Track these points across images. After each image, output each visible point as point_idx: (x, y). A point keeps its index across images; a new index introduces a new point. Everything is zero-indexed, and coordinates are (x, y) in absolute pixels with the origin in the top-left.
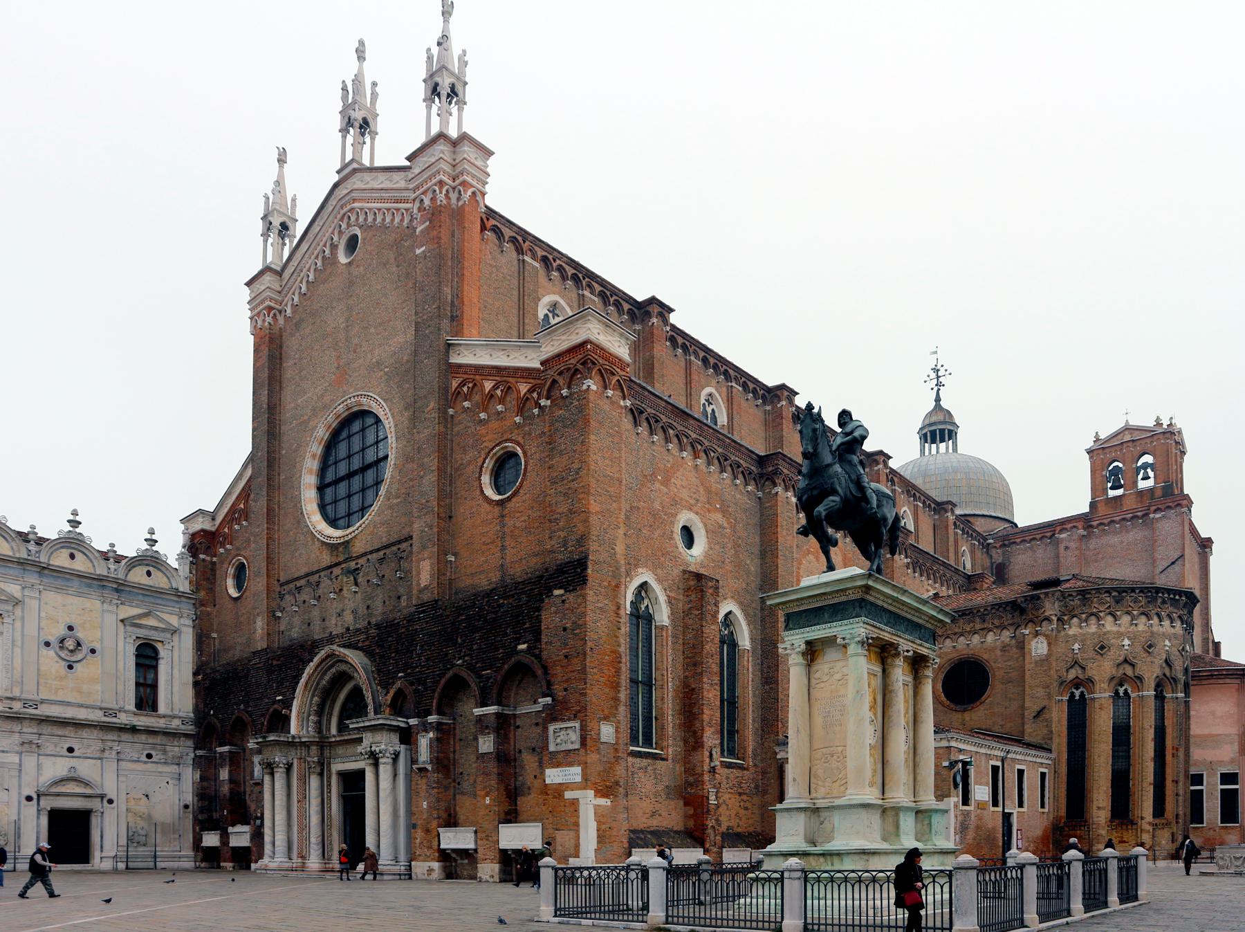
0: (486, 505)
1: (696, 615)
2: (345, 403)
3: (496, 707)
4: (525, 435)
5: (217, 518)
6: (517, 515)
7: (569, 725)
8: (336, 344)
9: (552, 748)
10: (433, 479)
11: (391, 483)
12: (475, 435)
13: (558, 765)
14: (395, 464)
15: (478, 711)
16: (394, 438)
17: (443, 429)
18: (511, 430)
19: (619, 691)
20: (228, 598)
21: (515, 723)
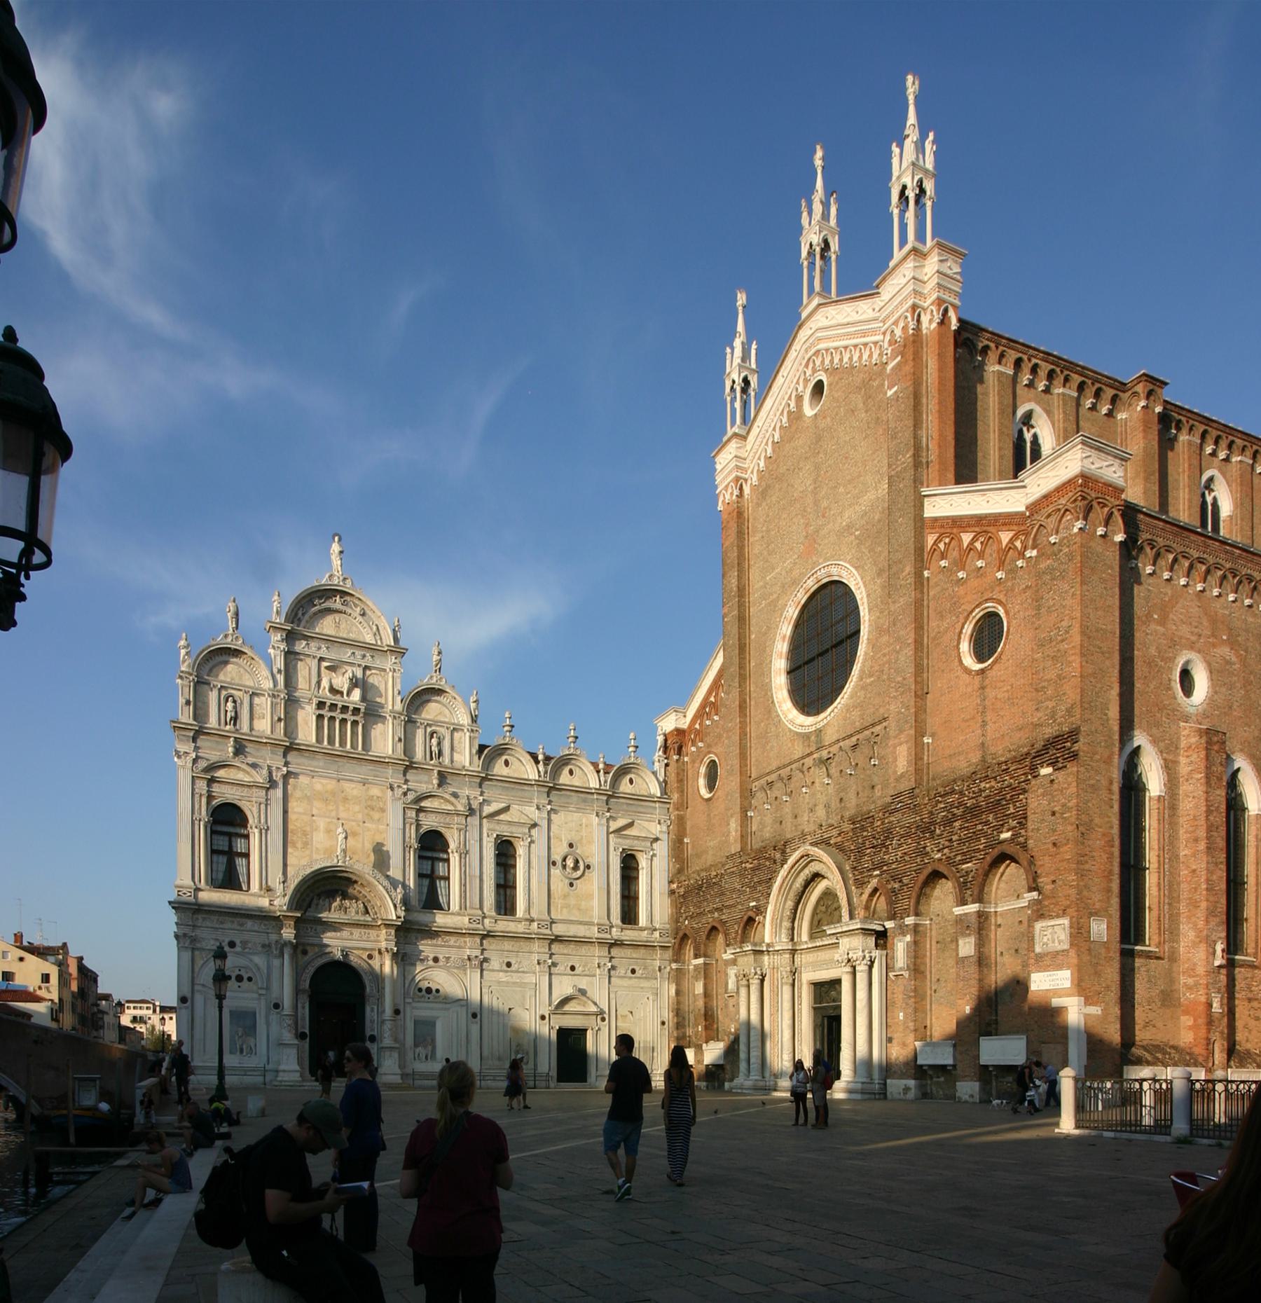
0: (966, 677)
1: (1198, 780)
2: (815, 576)
3: (977, 905)
4: (1007, 591)
5: (688, 714)
6: (999, 685)
7: (1057, 923)
8: (805, 511)
9: (1038, 949)
10: (909, 654)
11: (865, 660)
12: (953, 598)
13: (1046, 969)
14: (868, 639)
15: (959, 911)
16: (867, 610)
17: (919, 596)
18: (992, 587)
19: (1111, 881)
20: (700, 800)
21: (996, 922)
